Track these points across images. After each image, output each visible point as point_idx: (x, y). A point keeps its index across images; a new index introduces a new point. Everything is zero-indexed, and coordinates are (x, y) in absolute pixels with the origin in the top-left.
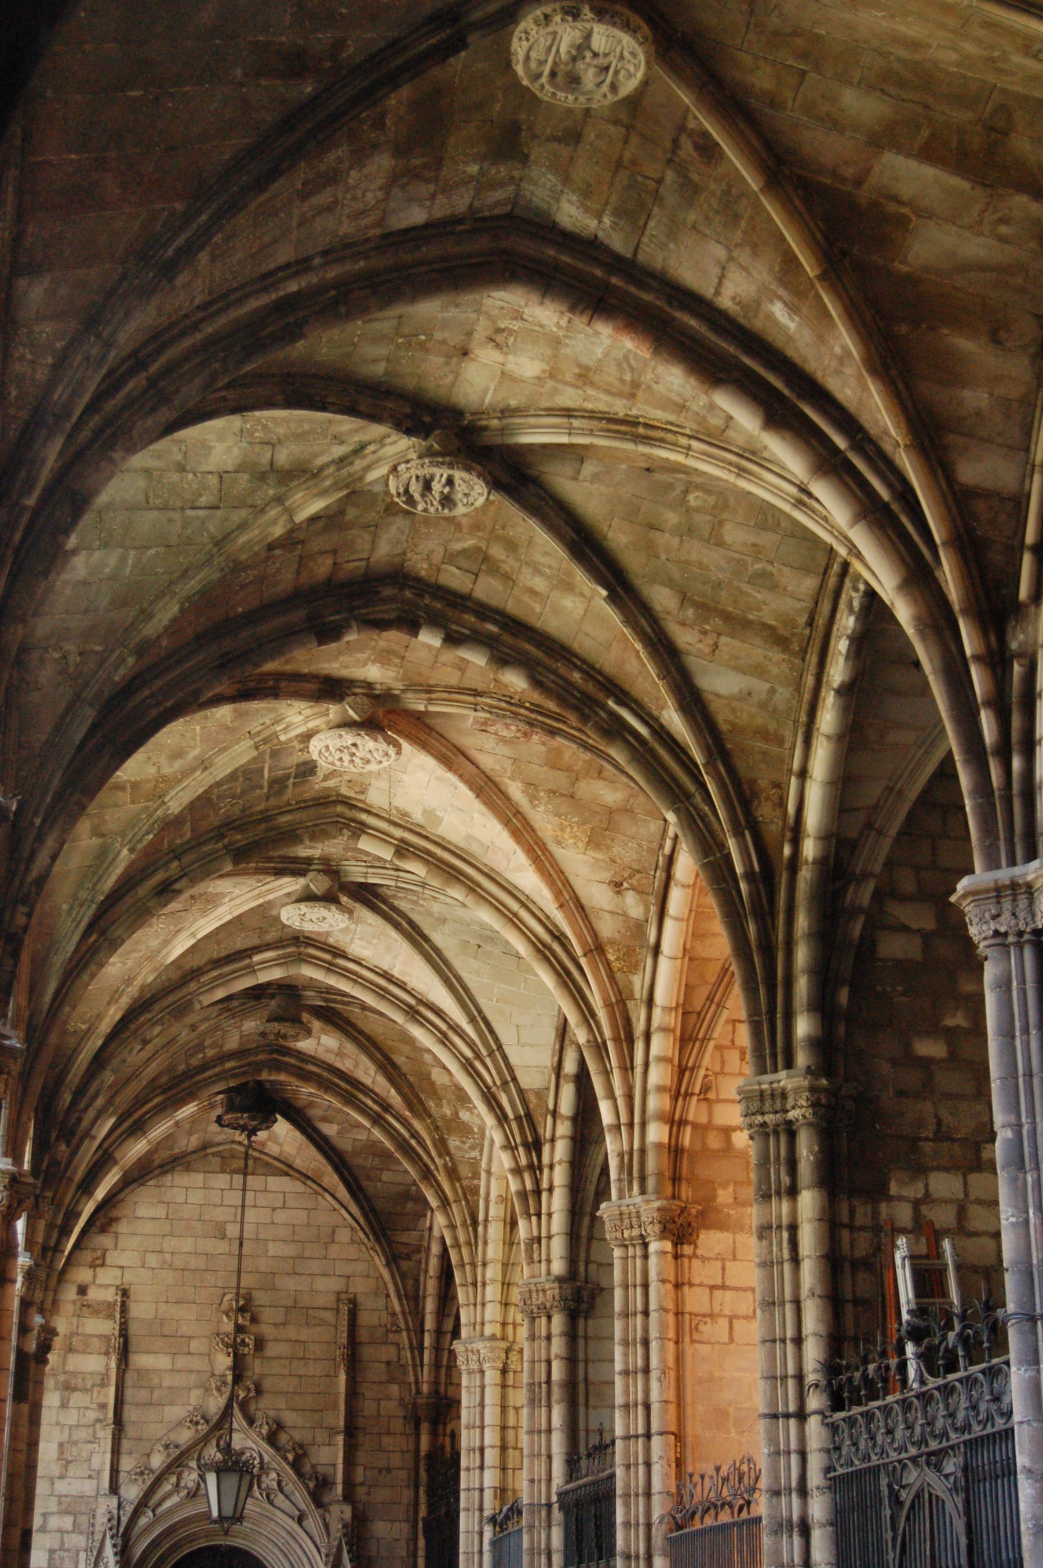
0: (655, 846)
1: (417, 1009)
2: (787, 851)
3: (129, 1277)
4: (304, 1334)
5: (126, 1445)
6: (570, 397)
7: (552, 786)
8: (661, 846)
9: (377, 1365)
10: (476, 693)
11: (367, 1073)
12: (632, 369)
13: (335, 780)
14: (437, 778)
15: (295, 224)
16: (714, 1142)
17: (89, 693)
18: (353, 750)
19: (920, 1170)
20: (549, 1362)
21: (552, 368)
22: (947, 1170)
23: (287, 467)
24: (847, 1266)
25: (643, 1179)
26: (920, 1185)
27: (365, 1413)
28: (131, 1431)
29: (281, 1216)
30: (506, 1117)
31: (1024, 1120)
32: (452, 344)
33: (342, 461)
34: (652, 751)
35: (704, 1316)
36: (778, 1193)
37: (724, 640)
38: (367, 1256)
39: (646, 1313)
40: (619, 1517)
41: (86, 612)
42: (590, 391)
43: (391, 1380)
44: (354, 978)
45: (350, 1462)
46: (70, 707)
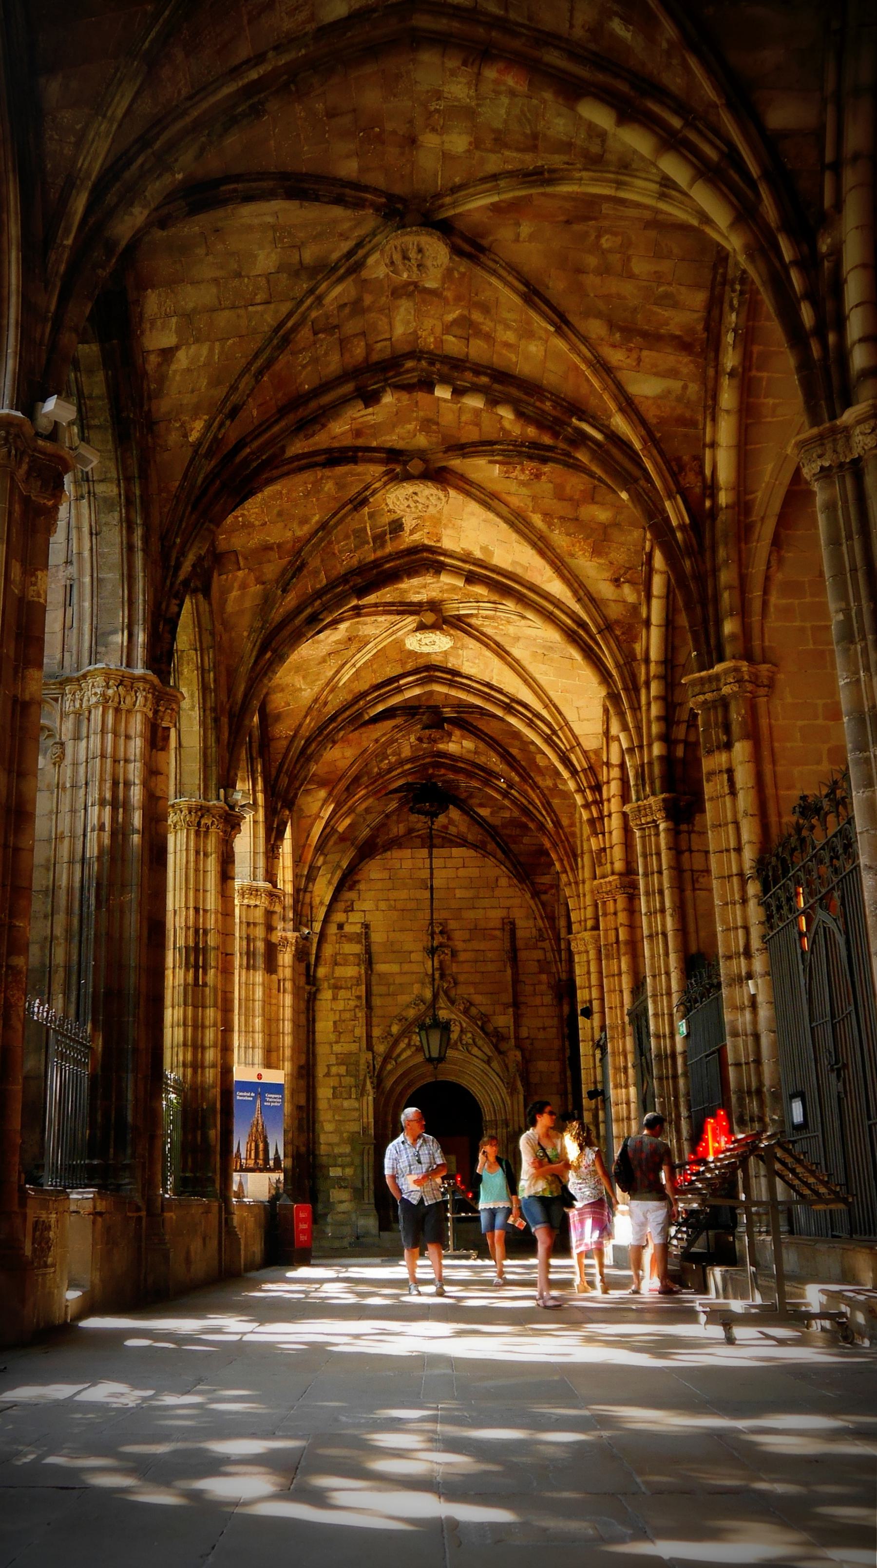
0: (639, 548)
1: (512, 705)
2: (708, 504)
3: (369, 917)
4: (482, 946)
5: (375, 1020)
6: (493, 163)
7: (562, 514)
8: (644, 548)
10: (491, 443)
11: (494, 761)
12: (528, 120)
13: (418, 534)
14: (484, 521)
15: (245, 21)
18: (415, 498)
20: (617, 929)
21: (475, 139)
28: (377, 1012)
29: (462, 872)
30: (576, 769)
32: (401, 133)
33: (351, 253)
34: (607, 452)
35: (702, 871)
37: (645, 353)
38: (519, 894)
39: (660, 872)
40: (651, 1012)
41: (193, 392)
42: (507, 153)
43: (540, 972)
45: (517, 1024)
46: (192, 460)
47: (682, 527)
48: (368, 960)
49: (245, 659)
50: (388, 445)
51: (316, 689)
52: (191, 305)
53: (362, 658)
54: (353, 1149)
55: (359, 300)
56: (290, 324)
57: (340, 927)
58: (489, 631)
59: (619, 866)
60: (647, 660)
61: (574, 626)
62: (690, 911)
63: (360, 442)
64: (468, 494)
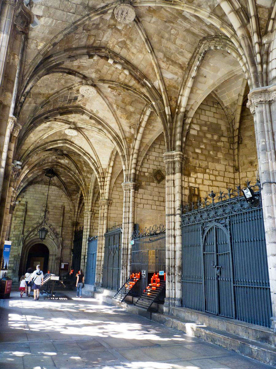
0: (138, 120)
2: (177, 110)
3: (28, 200)
4: (56, 211)
5: (25, 226)
8: (139, 120)
10: (113, 81)
11: (73, 167)
16: (142, 174)
17: (42, 53)
19: (196, 172)
20: (104, 213)
22: (201, 173)
23: (91, 6)
24: (184, 188)
25: (130, 179)
26: (196, 175)
28: (26, 224)
29: (53, 192)
31: (267, 141)
33: (103, 8)
34: (151, 90)
36: (171, 174)
39: (129, 202)
41: (43, 33)
43: (70, 219)
44: (75, 147)
45: (62, 231)
46: (37, 55)
47: (169, 115)
48: (26, 211)
49: (26, 124)
50: (84, 74)
51: (36, 138)
52: (50, 4)
53: (51, 133)
54: (14, 259)
55: (99, 24)
56: (79, 23)
57: (20, 202)
58: (85, 133)
59: (107, 198)
60: (134, 148)
61: (116, 136)
62: (136, 213)
63: (78, 70)
64: (100, 94)
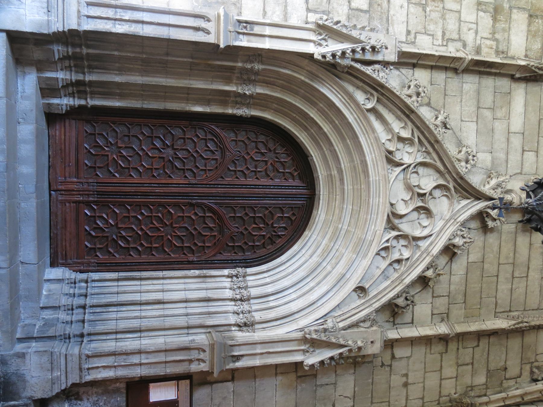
9: (504, 357)
27: (461, 350)
28: (454, 82)
